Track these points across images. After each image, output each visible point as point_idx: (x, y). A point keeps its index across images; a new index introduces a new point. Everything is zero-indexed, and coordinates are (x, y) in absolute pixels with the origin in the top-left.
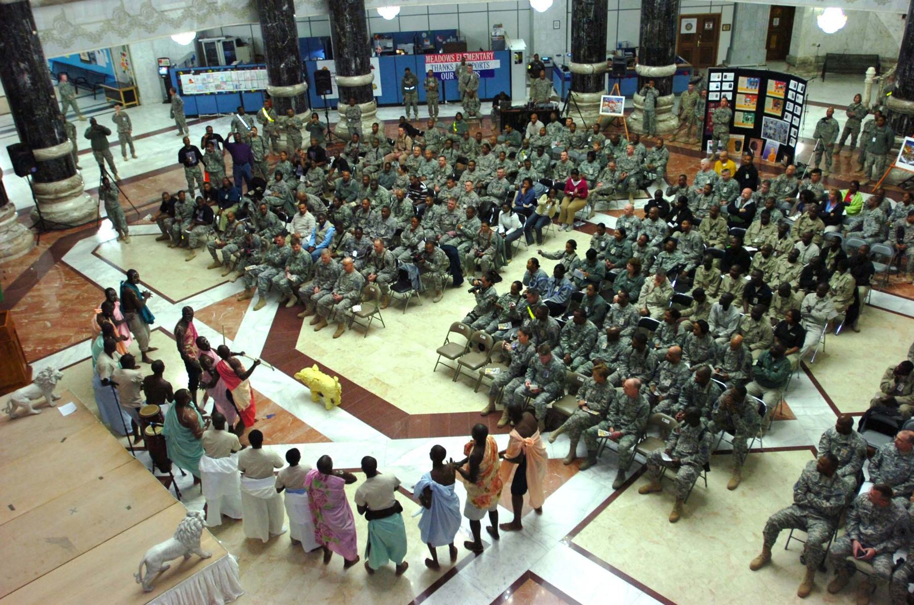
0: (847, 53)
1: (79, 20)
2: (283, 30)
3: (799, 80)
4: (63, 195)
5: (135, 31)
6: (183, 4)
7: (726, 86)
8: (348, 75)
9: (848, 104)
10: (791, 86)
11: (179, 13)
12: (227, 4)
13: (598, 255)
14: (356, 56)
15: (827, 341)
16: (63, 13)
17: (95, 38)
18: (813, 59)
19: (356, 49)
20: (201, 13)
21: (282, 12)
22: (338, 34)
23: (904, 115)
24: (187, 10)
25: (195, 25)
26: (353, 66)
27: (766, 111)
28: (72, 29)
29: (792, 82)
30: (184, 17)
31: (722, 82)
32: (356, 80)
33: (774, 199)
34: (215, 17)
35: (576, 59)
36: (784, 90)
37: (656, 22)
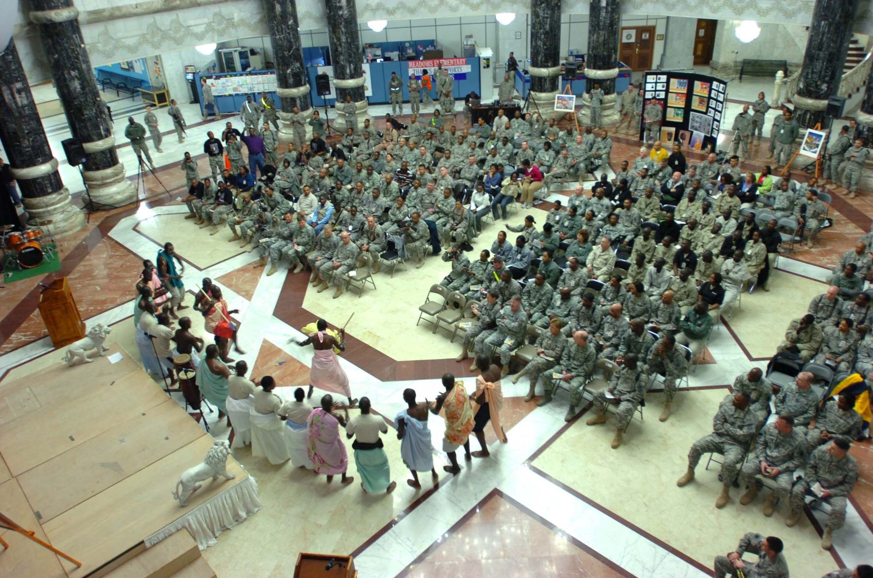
0: (760, 59)
1: (120, 35)
2: (289, 41)
3: (720, 82)
4: (108, 181)
5: (165, 44)
6: (206, 20)
7: (660, 87)
8: (344, 79)
9: (754, 101)
10: (714, 87)
11: (202, 28)
12: (242, 20)
13: (553, 229)
14: (350, 62)
15: (742, 299)
16: (106, 29)
17: (132, 49)
18: (732, 64)
19: (350, 56)
20: (220, 28)
21: (288, 26)
22: (335, 44)
23: (807, 111)
24: (209, 25)
25: (216, 38)
26: (348, 71)
27: (693, 108)
28: (114, 42)
29: (715, 83)
30: (207, 31)
31: (656, 83)
32: (351, 83)
33: (699, 181)
34: (232, 31)
35: (535, 64)
36: (708, 90)
37: (602, 33)
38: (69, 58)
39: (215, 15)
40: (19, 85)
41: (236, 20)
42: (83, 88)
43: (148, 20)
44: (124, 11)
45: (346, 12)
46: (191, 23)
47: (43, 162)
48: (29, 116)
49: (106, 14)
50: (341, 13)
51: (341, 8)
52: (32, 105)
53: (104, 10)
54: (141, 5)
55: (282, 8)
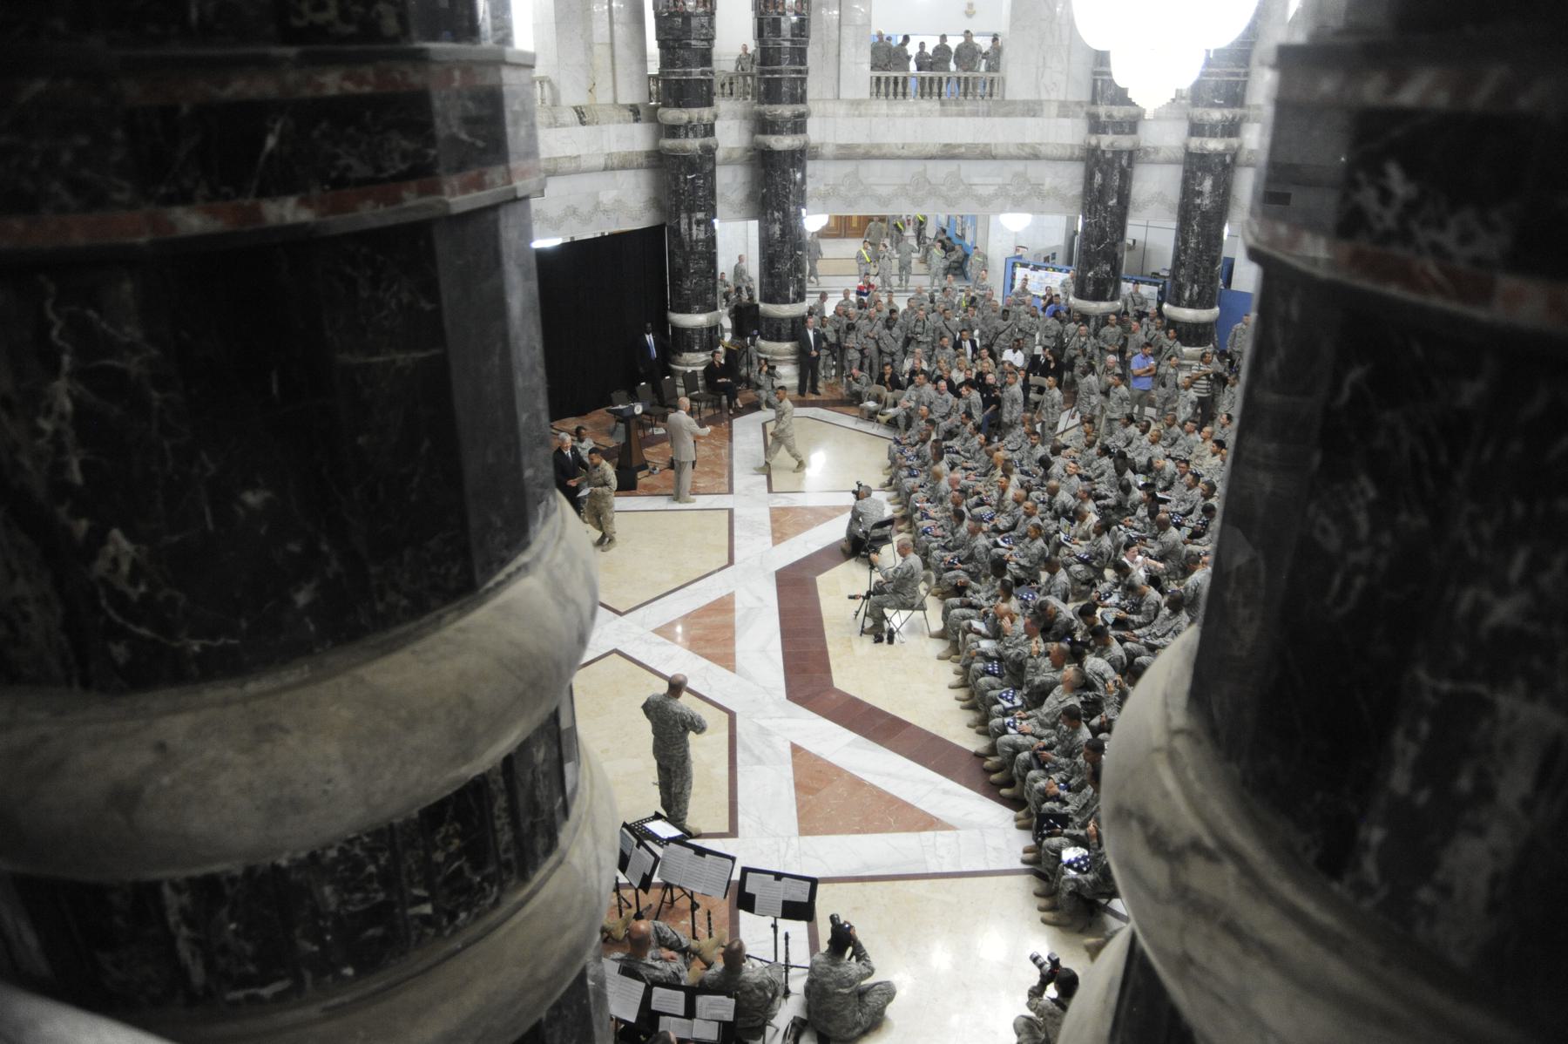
2: (1102, 230)
6: (999, 181)
11: (991, 190)
14: (1194, 282)
17: (885, 202)
19: (1196, 272)
20: (1019, 194)
26: (1187, 294)
30: (996, 196)
38: (777, 195)
39: (1016, 175)
40: (700, 215)
41: (1047, 187)
42: (783, 234)
43: (917, 166)
44: (885, 151)
45: (1207, 202)
46: (976, 180)
47: (699, 312)
48: (701, 253)
49: (861, 151)
50: (1198, 201)
51: (1200, 194)
52: (711, 241)
53: (859, 146)
54: (910, 145)
55: (1104, 180)
